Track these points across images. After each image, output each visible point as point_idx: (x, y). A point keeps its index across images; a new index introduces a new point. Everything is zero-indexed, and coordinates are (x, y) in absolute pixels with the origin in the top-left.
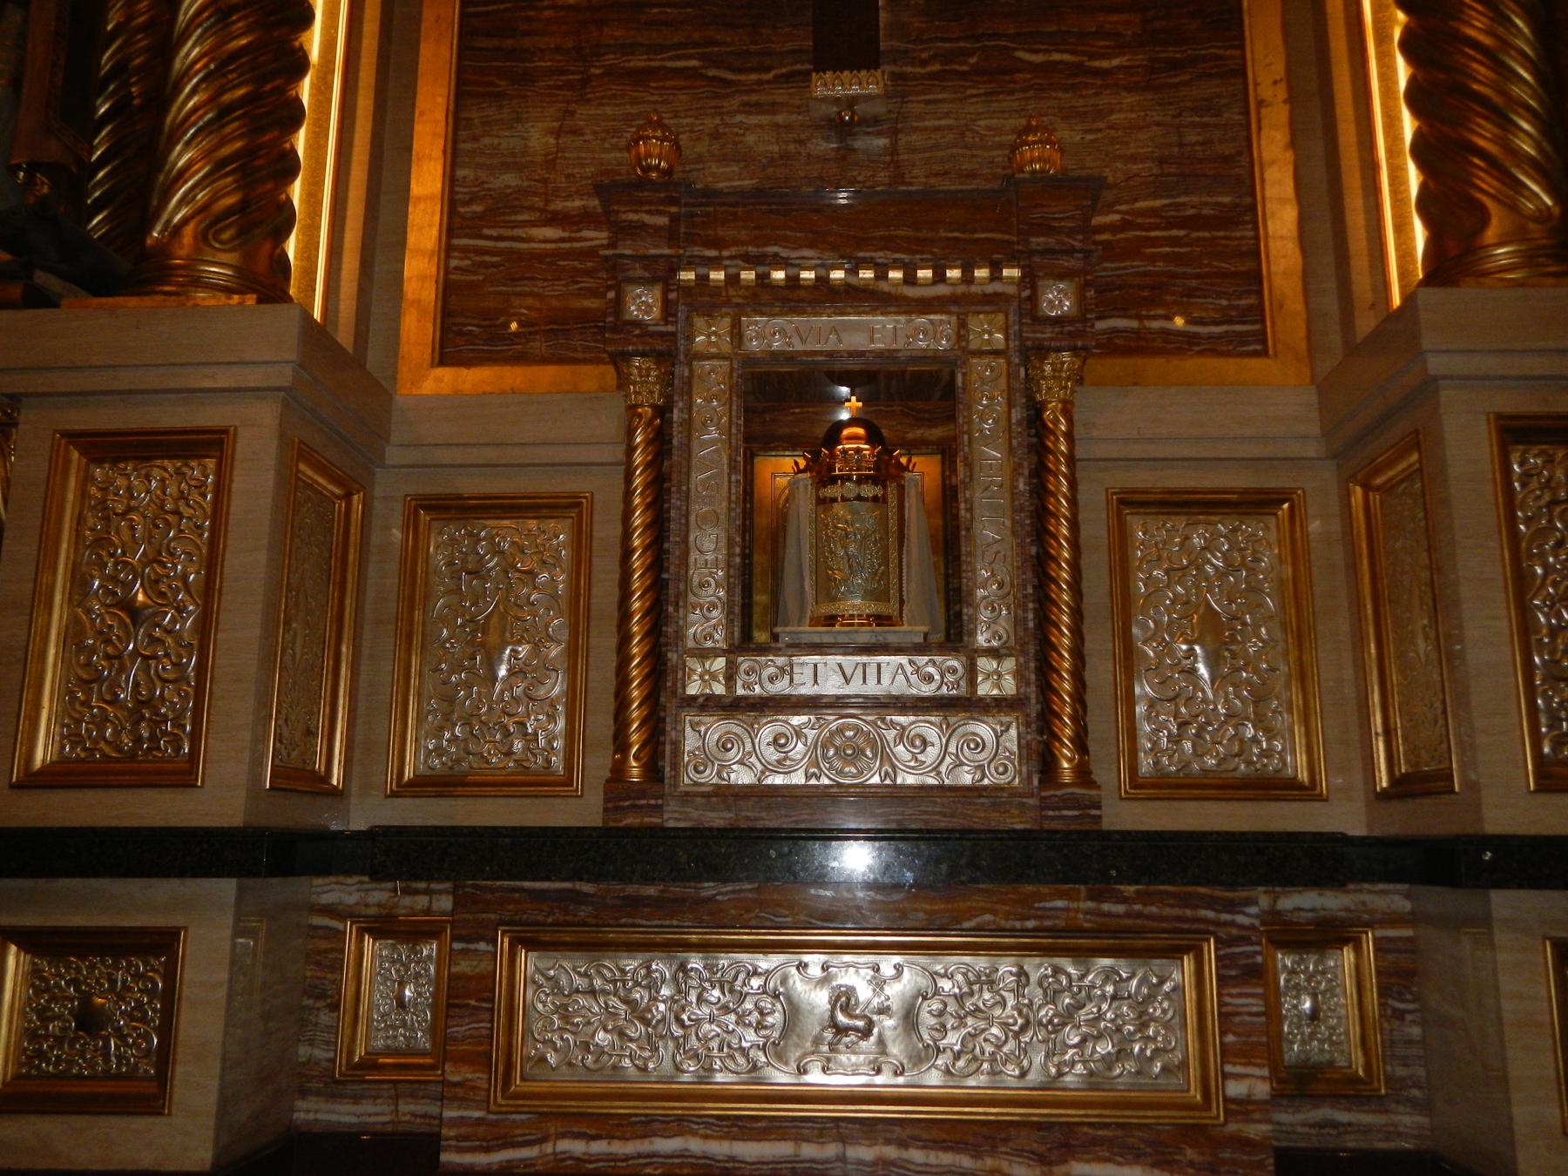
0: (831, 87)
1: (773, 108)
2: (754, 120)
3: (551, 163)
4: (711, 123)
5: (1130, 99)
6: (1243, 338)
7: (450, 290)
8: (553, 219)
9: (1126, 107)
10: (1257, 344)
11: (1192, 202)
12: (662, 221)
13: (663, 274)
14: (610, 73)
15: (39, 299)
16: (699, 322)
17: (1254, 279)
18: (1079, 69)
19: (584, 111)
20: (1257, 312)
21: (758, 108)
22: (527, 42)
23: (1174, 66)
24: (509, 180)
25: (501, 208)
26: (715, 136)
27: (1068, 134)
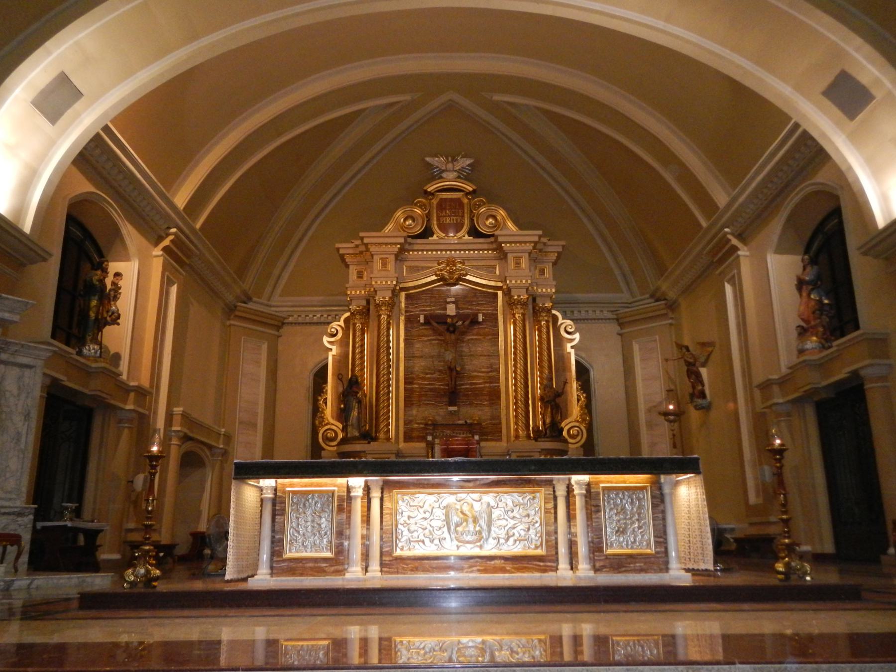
0: (451, 408)
1: (443, 409)
2: (442, 410)
3: (416, 416)
4: (435, 411)
5: (487, 408)
6: (499, 439)
7: (405, 433)
8: (417, 423)
9: (487, 409)
10: (500, 440)
11: (494, 422)
12: (431, 428)
13: (432, 434)
14: (423, 404)
15: (369, 443)
16: (436, 440)
17: (501, 432)
18: (481, 404)
19: (420, 409)
20: (501, 436)
21: (441, 409)
22: (413, 399)
23: (493, 404)
24: (410, 418)
25: (410, 422)
26: (437, 412)
27: (480, 413)
